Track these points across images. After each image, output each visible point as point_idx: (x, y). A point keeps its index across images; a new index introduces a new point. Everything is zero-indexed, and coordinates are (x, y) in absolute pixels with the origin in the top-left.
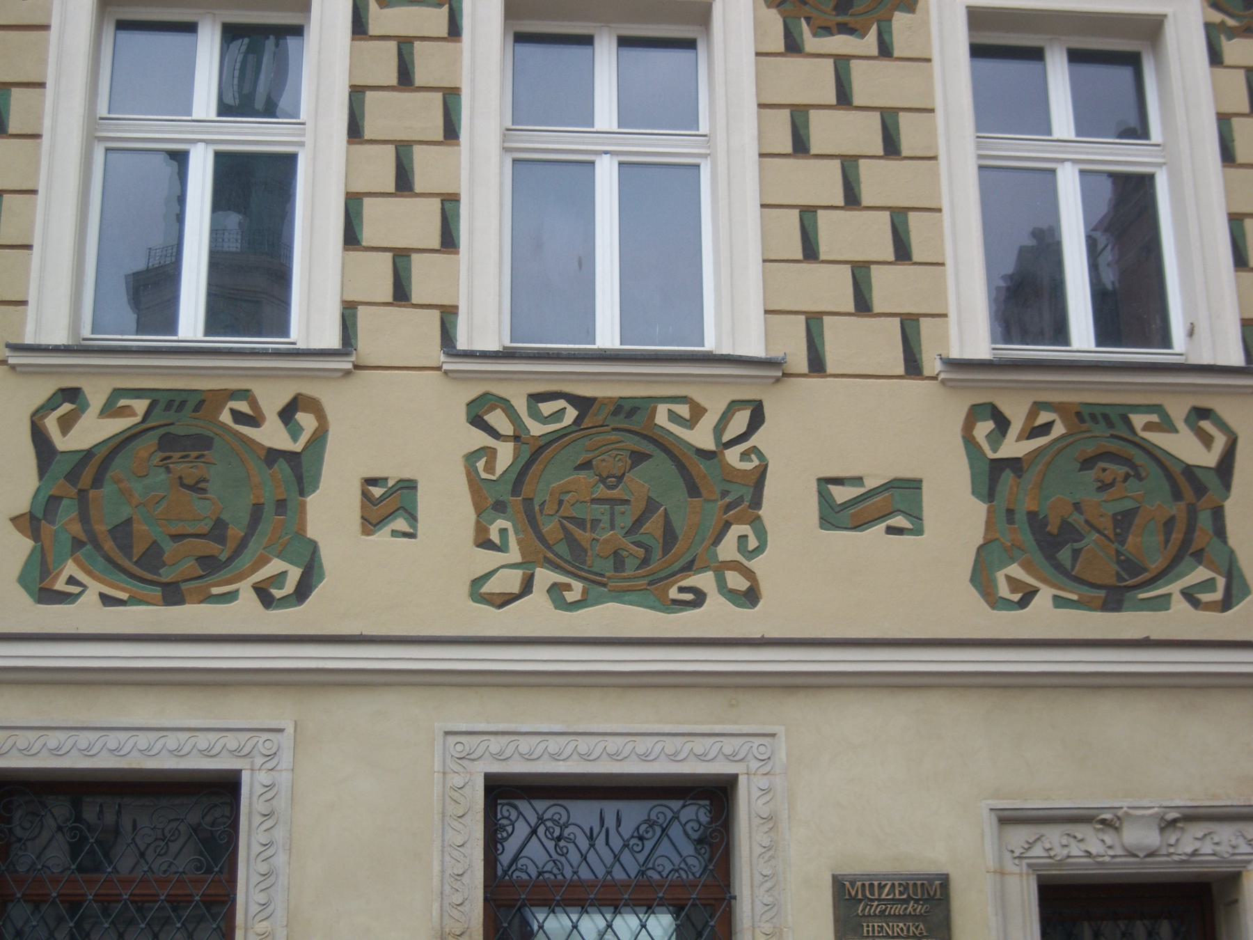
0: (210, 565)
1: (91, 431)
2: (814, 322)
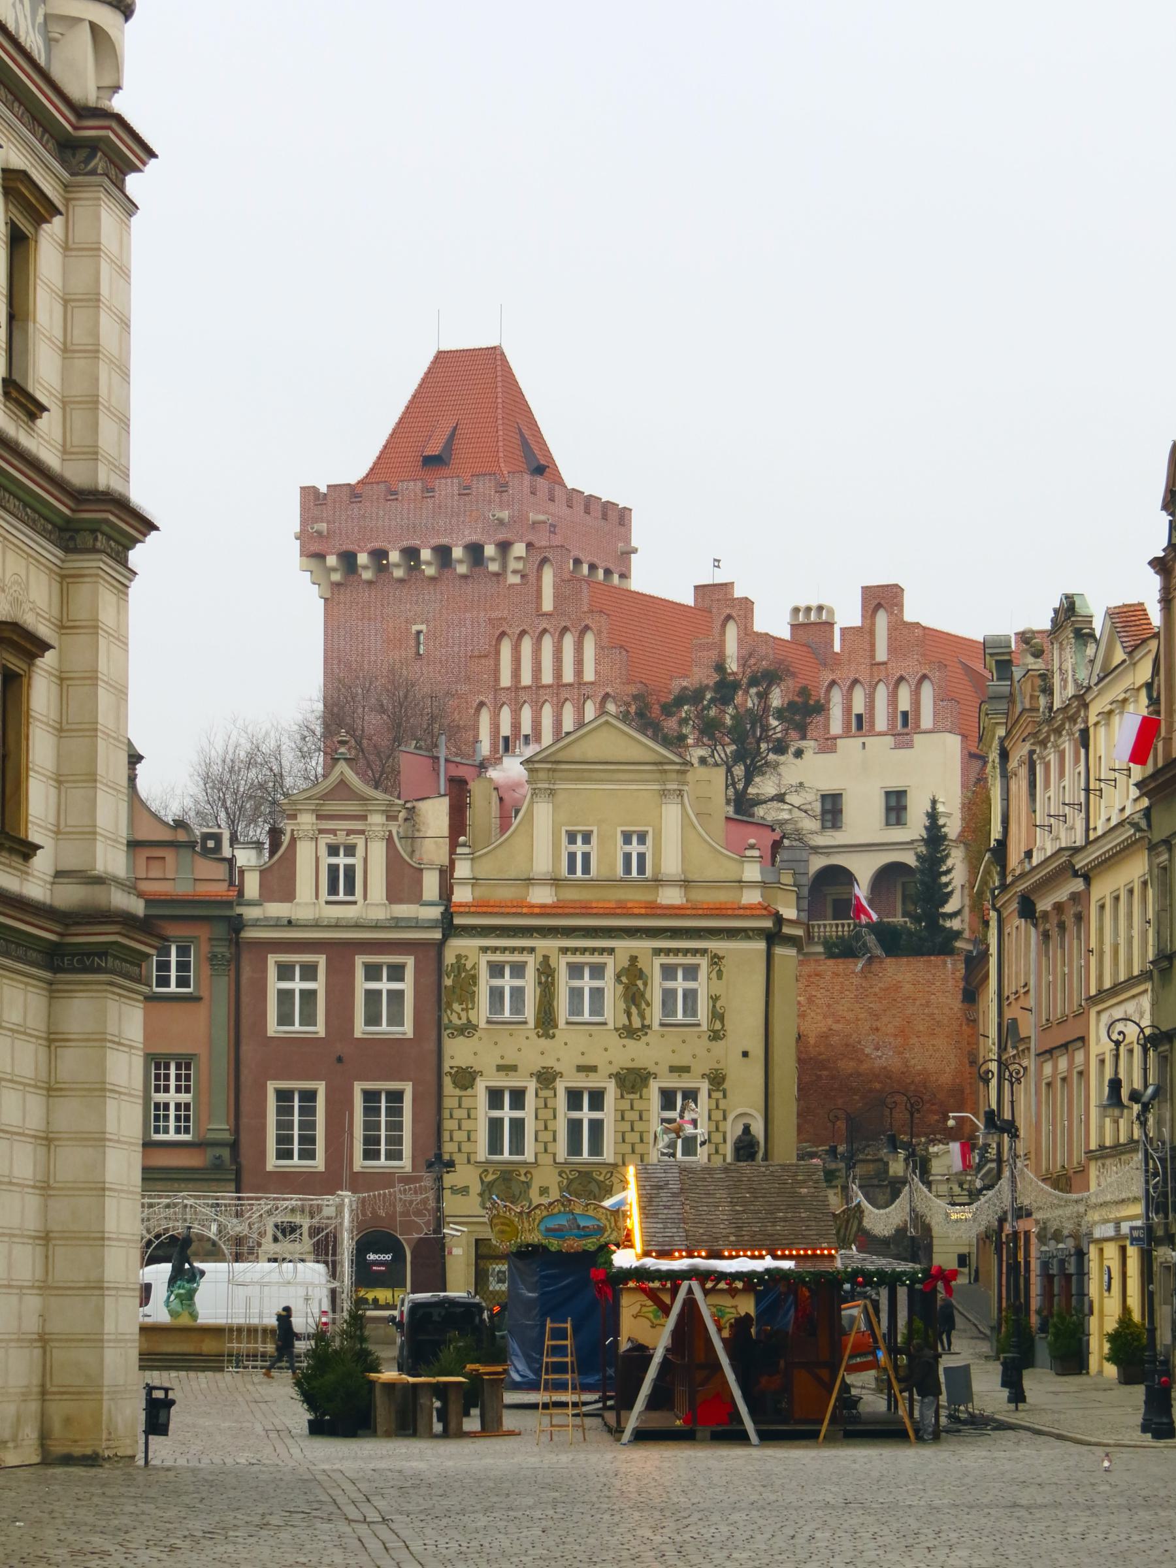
1: (490, 1178)
2: (623, 1155)
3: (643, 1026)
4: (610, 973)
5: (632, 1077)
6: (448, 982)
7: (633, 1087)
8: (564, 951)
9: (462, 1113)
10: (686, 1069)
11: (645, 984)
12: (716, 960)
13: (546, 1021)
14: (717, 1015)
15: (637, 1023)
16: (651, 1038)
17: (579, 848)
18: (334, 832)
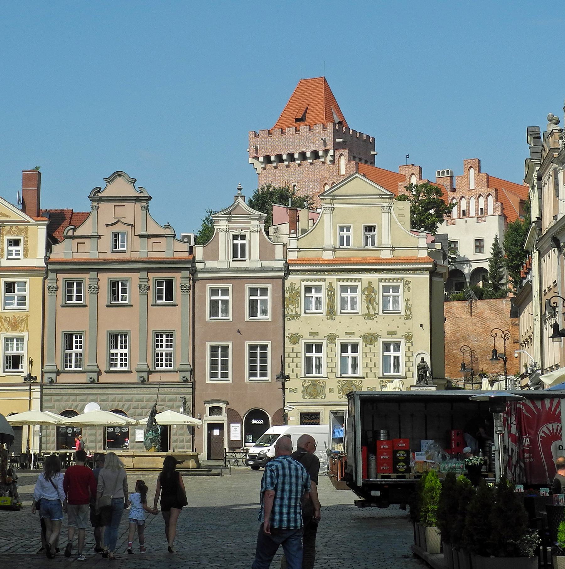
0: (317, 395)
1: (307, 384)
3: (375, 314)
4: (359, 290)
5: (370, 337)
6: (287, 295)
7: (371, 342)
8: (339, 280)
9: (293, 355)
10: (395, 333)
11: (375, 295)
12: (407, 283)
13: (331, 312)
14: (408, 308)
15: (372, 312)
16: (379, 319)
17: (345, 233)
18: (236, 229)
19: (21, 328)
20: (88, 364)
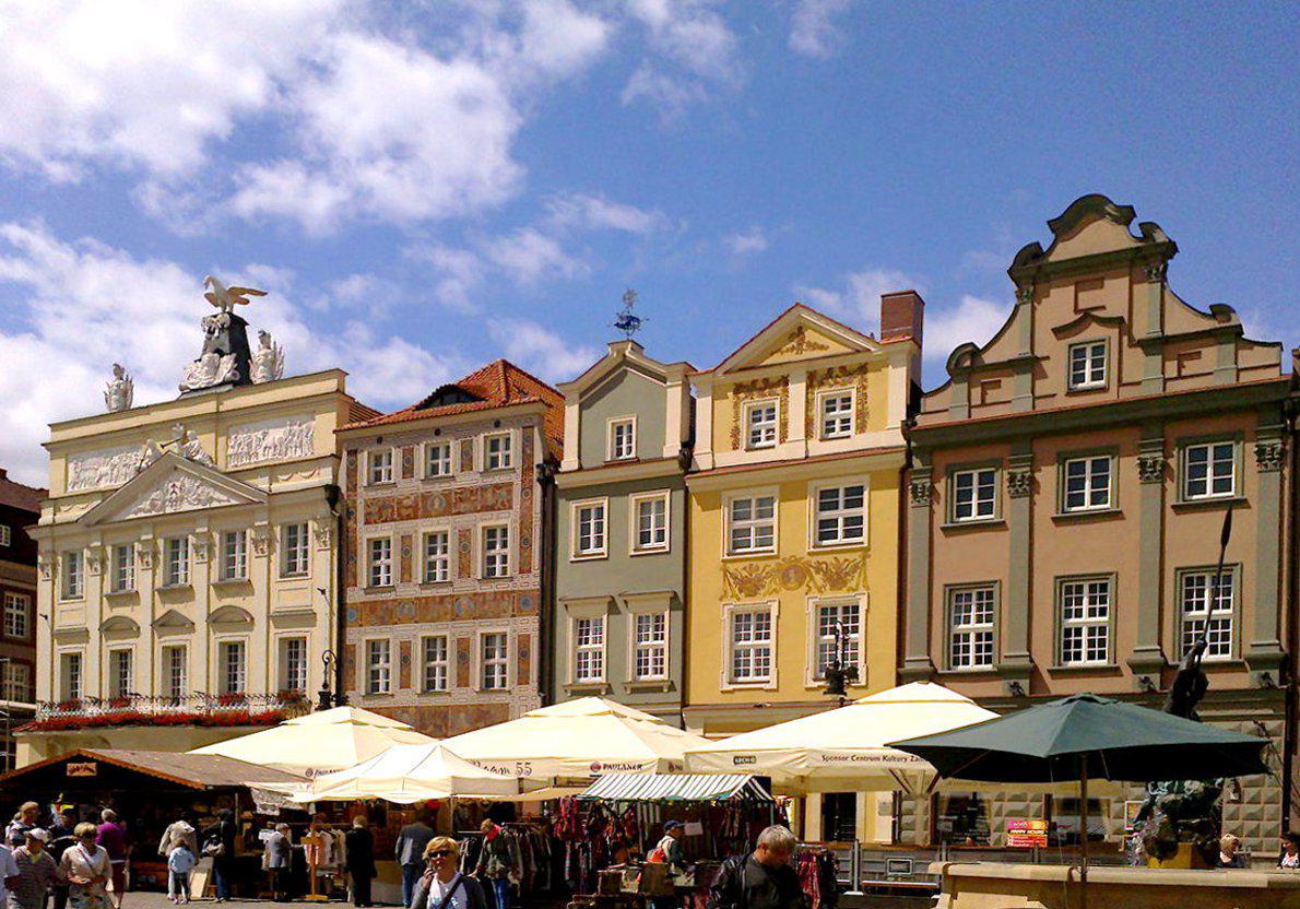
19: (852, 584)
20: (1010, 652)
